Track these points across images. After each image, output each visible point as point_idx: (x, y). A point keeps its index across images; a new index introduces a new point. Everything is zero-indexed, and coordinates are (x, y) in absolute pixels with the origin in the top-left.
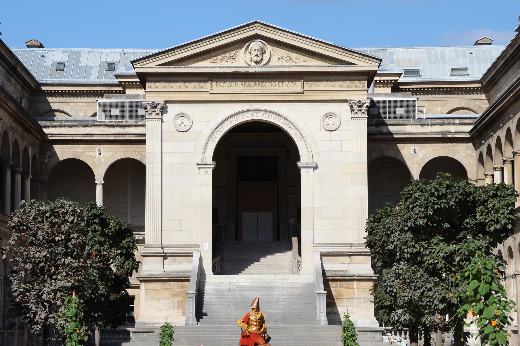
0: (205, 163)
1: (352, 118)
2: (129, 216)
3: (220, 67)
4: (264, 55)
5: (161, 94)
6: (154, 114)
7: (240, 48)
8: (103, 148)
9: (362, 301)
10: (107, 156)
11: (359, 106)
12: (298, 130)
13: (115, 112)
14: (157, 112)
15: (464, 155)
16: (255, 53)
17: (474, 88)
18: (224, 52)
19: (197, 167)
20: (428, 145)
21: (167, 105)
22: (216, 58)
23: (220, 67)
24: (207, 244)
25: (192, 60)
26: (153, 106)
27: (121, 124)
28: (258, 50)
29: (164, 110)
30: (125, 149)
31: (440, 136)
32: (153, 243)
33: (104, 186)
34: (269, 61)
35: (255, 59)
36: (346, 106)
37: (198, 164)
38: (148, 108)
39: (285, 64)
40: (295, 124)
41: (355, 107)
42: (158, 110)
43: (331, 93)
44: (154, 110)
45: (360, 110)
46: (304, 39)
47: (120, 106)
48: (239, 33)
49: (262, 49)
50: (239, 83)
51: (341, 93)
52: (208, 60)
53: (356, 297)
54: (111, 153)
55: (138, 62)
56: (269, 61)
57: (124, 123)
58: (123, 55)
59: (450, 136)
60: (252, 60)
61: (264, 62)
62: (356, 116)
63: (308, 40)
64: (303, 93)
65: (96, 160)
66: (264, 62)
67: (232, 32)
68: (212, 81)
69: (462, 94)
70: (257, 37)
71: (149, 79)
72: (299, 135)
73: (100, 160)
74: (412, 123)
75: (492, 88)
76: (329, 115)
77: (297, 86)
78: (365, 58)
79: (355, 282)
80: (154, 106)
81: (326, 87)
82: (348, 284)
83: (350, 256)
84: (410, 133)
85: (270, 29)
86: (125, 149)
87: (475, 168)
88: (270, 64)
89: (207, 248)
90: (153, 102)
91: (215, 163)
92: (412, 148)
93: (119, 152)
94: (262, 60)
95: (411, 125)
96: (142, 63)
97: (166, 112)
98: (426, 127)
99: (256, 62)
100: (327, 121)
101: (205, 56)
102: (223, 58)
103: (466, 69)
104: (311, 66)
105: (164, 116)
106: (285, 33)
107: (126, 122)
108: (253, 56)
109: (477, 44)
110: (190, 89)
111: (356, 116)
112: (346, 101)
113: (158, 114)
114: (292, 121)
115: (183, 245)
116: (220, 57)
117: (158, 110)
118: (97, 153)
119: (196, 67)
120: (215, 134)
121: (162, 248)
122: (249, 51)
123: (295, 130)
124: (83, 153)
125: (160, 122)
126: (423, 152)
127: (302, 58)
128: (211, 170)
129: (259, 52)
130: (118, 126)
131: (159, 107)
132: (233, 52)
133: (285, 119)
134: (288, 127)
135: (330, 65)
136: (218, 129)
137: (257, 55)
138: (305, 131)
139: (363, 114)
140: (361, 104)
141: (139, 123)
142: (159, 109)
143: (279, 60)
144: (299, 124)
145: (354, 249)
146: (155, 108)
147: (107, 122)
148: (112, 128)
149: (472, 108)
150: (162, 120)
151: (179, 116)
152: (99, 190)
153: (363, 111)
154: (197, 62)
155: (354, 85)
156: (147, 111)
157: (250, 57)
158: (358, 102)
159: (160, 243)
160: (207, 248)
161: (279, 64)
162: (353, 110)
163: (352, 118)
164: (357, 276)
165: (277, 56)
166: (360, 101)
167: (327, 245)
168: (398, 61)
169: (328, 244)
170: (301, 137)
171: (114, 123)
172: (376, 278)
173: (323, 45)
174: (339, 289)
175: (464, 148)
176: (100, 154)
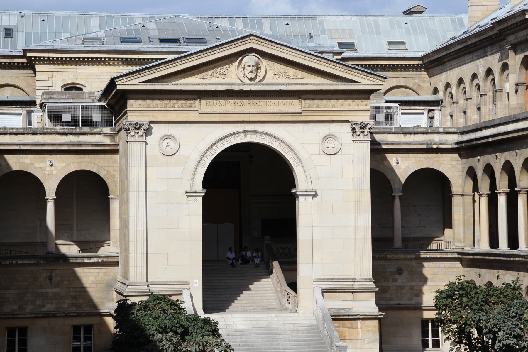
0: (194, 190)
1: (353, 141)
2: (75, 229)
3: (212, 84)
4: (259, 71)
5: (145, 114)
6: (137, 135)
7: (232, 62)
8: (55, 159)
9: (366, 342)
10: (59, 168)
11: (361, 128)
12: (295, 154)
13: (67, 117)
14: (141, 134)
15: (449, 166)
16: (250, 68)
17: (414, 65)
18: (215, 67)
19: (185, 195)
20: (411, 155)
21: (151, 124)
22: (206, 73)
23: (212, 84)
24: (197, 280)
25: (179, 76)
26: (137, 127)
27: (74, 131)
28: (253, 66)
29: (148, 132)
30: (79, 160)
31: (425, 146)
32: (138, 281)
33: (57, 202)
34: (264, 78)
35: (250, 75)
36: (347, 127)
37: (186, 192)
38: (131, 129)
39: (281, 81)
40: (292, 147)
41: (357, 128)
42: (141, 131)
43: (331, 113)
44: (137, 131)
45: (363, 132)
46: (304, 54)
47: (73, 110)
48: (232, 47)
49: (257, 64)
50: (232, 101)
51: (342, 113)
52: (196, 76)
53: (360, 337)
54: (63, 165)
55: (120, 79)
56: (264, 78)
57: (78, 130)
58: (20, 18)
59: (435, 146)
60: (245, 76)
61: (258, 79)
62: (358, 138)
63: (308, 55)
64: (301, 113)
65: (47, 173)
66: (258, 79)
67: (225, 46)
68: (201, 99)
69: (401, 71)
70: (251, 51)
71: (132, 96)
72: (297, 160)
73: (51, 173)
74: (393, 131)
75: (435, 66)
76: (329, 137)
77: (295, 105)
78: (370, 75)
79: (359, 321)
80: (138, 126)
81: (325, 106)
82: (352, 324)
83: (353, 292)
84: (392, 144)
85: (267, 42)
86: (79, 160)
87: (460, 181)
88: (265, 82)
89: (197, 285)
90: (137, 123)
91: (205, 191)
92: (394, 158)
93: (73, 163)
94: (256, 76)
95: (393, 133)
96: (125, 79)
97: (151, 133)
98: (408, 135)
99: (251, 79)
100: (327, 143)
101: (193, 72)
102: (213, 73)
103: (403, 43)
104: (311, 84)
105: (149, 137)
106: (283, 47)
107: (80, 129)
108: (247, 72)
109: (409, 12)
110: (177, 108)
111: (358, 138)
112: (348, 122)
113: (142, 136)
114: (290, 144)
115: (171, 282)
116: (210, 73)
117: (141, 131)
118: (48, 165)
119: (185, 85)
120: (205, 158)
121: (148, 286)
122: (242, 66)
123: (292, 154)
124: (32, 164)
125: (144, 145)
126: (406, 163)
127: (300, 73)
128: (201, 198)
129: (254, 68)
130: (71, 134)
131: (142, 128)
132: (225, 67)
133: (282, 141)
134: (284, 150)
135: (334, 83)
136: (209, 152)
137: (252, 72)
138: (303, 154)
139: (365, 137)
140: (364, 125)
141: (95, 131)
142: (143, 131)
143: (275, 77)
144: (296, 146)
145: (357, 285)
146: (138, 129)
147: (58, 128)
148: (64, 137)
149: (411, 86)
150: (145, 142)
151: (164, 138)
152: (50, 207)
153: (366, 133)
154: (184, 77)
155: (356, 105)
156: (130, 133)
157: (243, 73)
158: (361, 124)
159: (146, 280)
160: (197, 285)
161: (274, 81)
162: (355, 132)
163: (353, 141)
164: (361, 315)
165: (272, 71)
166: (362, 122)
167: (328, 280)
168: (330, 31)
169: (328, 279)
170: (299, 162)
171: (66, 131)
172: (382, 317)
173: (324, 61)
174: (341, 329)
175: (449, 159)
176: (51, 165)
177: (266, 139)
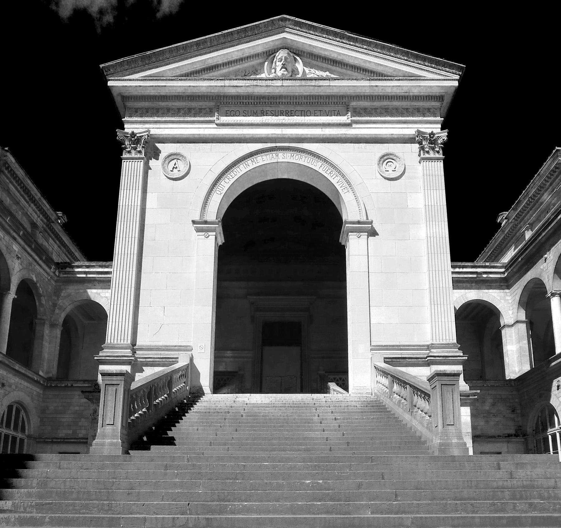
12: (343, 176)
19: (192, 228)
37: (194, 222)
62: (427, 156)
72: (345, 184)
111: (427, 156)
123: (339, 178)
138: (353, 178)
146: (137, 144)
177: (304, 159)
